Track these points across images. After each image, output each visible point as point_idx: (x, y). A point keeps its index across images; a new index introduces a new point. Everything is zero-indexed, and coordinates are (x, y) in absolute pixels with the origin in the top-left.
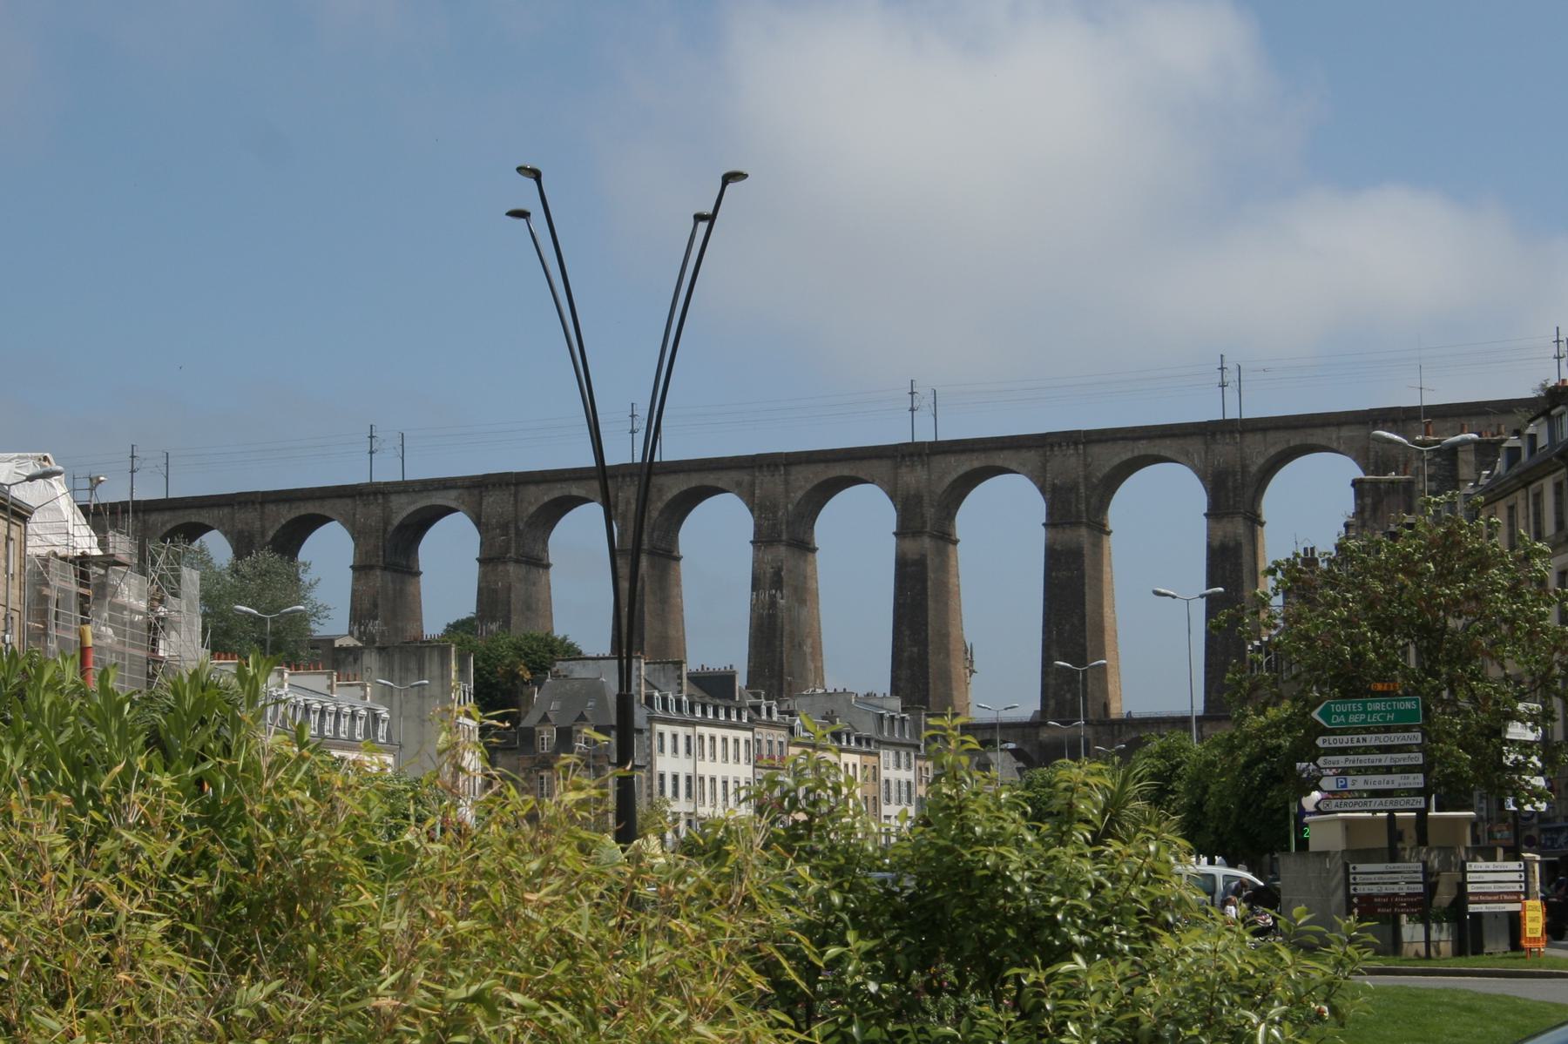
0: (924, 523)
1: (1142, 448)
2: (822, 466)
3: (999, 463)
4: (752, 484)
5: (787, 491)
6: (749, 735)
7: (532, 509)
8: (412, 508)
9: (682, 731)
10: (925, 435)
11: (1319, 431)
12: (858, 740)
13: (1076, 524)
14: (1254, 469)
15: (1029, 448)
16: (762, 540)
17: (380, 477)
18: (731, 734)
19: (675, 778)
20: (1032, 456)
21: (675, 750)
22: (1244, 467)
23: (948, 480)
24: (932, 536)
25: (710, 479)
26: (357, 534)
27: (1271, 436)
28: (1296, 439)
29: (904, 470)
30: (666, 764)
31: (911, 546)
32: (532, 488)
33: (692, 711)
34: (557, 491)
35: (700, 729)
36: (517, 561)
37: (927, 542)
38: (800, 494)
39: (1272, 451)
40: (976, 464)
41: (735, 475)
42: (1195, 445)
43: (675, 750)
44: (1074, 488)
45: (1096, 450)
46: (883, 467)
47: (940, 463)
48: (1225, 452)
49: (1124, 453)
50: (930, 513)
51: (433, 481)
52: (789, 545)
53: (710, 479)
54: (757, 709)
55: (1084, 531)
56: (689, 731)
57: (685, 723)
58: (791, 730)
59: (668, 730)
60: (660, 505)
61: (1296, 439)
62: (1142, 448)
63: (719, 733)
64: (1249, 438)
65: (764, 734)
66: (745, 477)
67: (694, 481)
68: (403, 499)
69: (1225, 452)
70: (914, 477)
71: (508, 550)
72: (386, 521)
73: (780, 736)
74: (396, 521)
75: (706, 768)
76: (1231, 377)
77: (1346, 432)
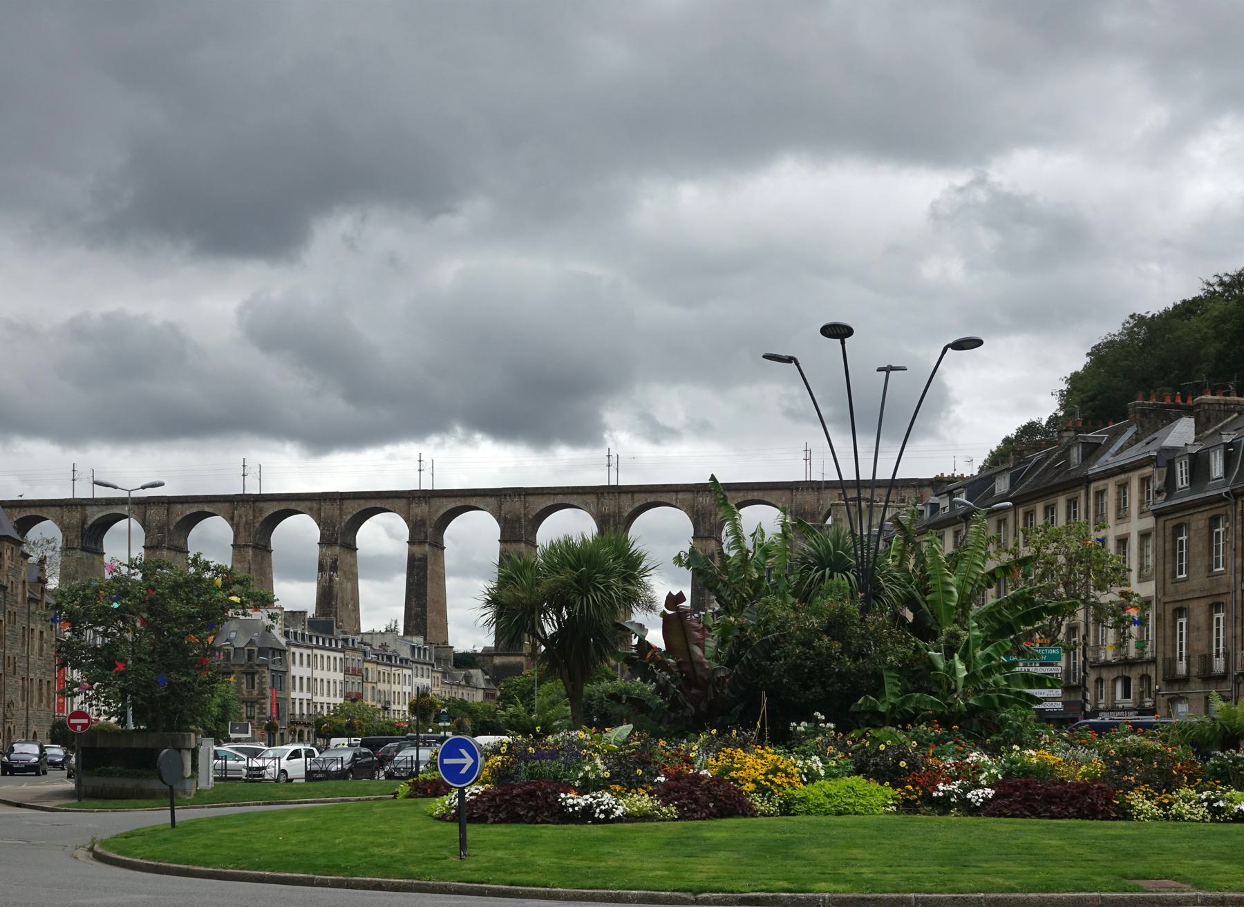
0: (426, 537)
1: (559, 499)
2: (362, 502)
3: (472, 504)
4: (320, 509)
5: (341, 515)
6: (342, 655)
7: (179, 518)
8: (100, 515)
9: (306, 652)
10: (426, 486)
11: (665, 495)
12: (401, 660)
13: (519, 541)
14: (626, 514)
15: (491, 496)
16: (325, 542)
17: (78, 495)
18: (332, 654)
19: (301, 678)
20: (492, 501)
21: (301, 663)
22: (620, 513)
23: (441, 512)
24: (430, 544)
25: (292, 506)
26: (64, 529)
27: (636, 496)
28: (651, 498)
29: (414, 505)
30: (296, 670)
31: (418, 550)
32: (179, 506)
33: (311, 640)
34: (194, 509)
35: (316, 651)
36: (169, 549)
37: (427, 547)
38: (349, 517)
39: (637, 505)
40: (459, 504)
41: (308, 504)
42: (592, 499)
43: (301, 663)
44: (518, 520)
45: (531, 499)
46: (402, 503)
47: (436, 502)
48: (608, 505)
49: (549, 502)
50: (430, 530)
51: (114, 499)
52: (341, 546)
53: (292, 506)
54: (346, 640)
55: (523, 545)
56: (309, 652)
57: (307, 647)
58: (365, 654)
59: (298, 651)
60: (261, 519)
61: (651, 498)
62: (559, 499)
63: (326, 654)
64: (623, 497)
65: (350, 655)
66: (315, 505)
67: (283, 506)
68: (95, 509)
69: (608, 505)
70: (420, 510)
71: (163, 542)
72: (84, 522)
73: (359, 656)
74: (90, 523)
75: (318, 674)
76: (613, 461)
77: (680, 496)
